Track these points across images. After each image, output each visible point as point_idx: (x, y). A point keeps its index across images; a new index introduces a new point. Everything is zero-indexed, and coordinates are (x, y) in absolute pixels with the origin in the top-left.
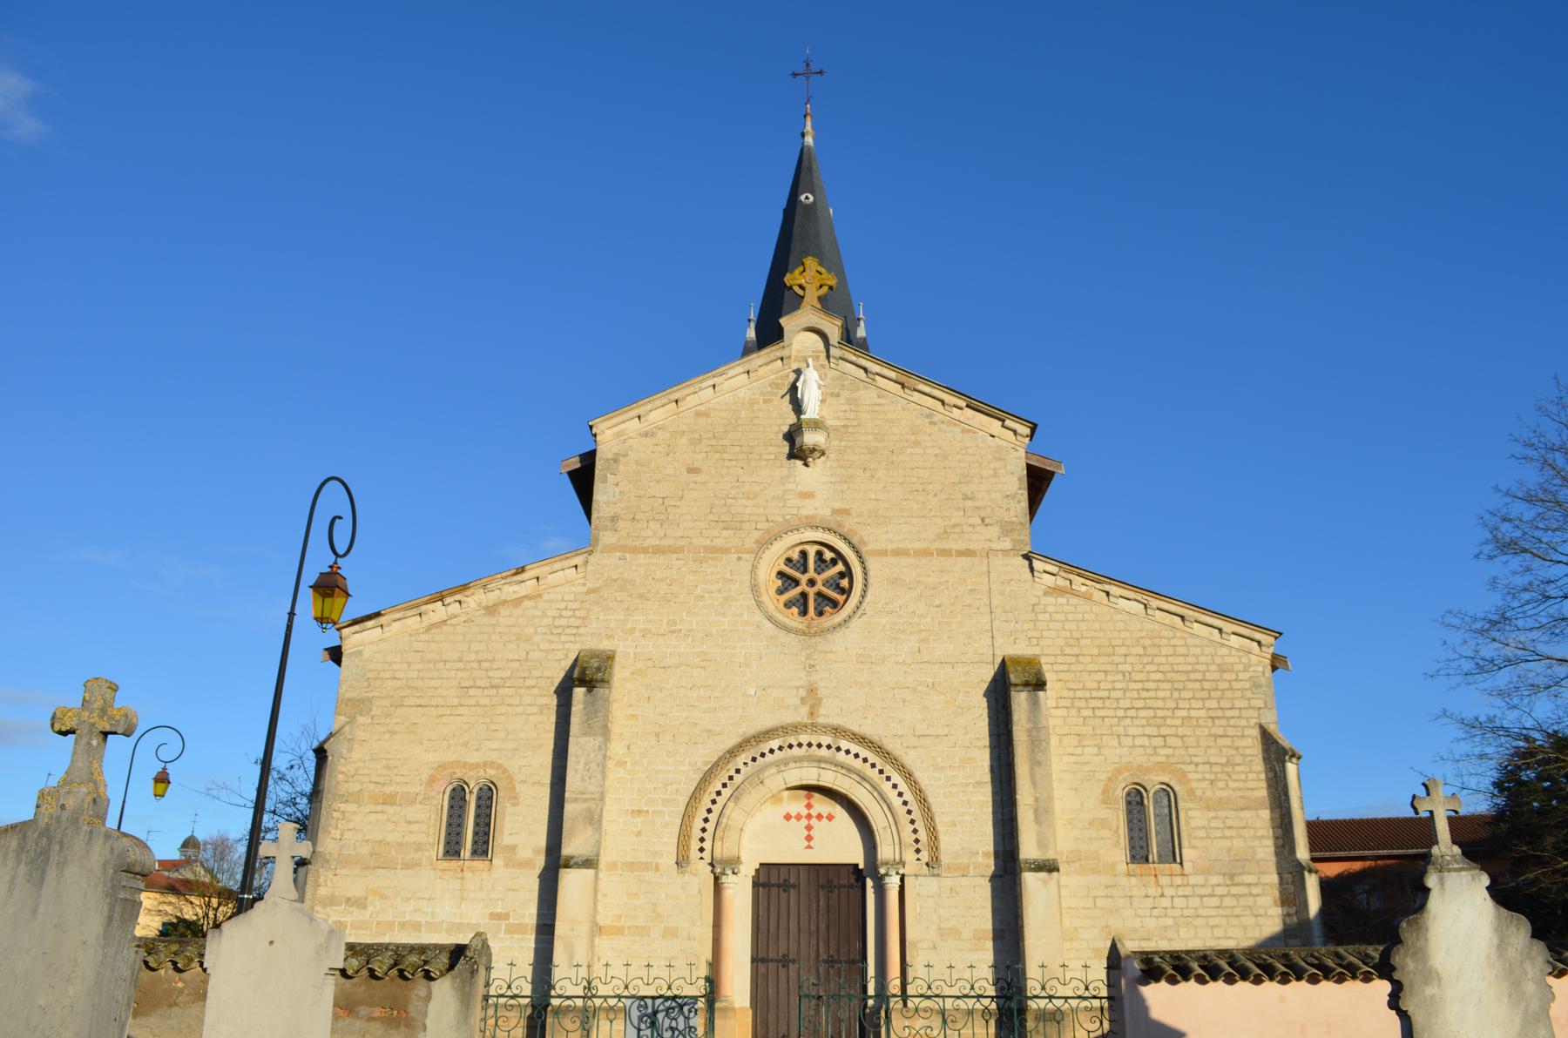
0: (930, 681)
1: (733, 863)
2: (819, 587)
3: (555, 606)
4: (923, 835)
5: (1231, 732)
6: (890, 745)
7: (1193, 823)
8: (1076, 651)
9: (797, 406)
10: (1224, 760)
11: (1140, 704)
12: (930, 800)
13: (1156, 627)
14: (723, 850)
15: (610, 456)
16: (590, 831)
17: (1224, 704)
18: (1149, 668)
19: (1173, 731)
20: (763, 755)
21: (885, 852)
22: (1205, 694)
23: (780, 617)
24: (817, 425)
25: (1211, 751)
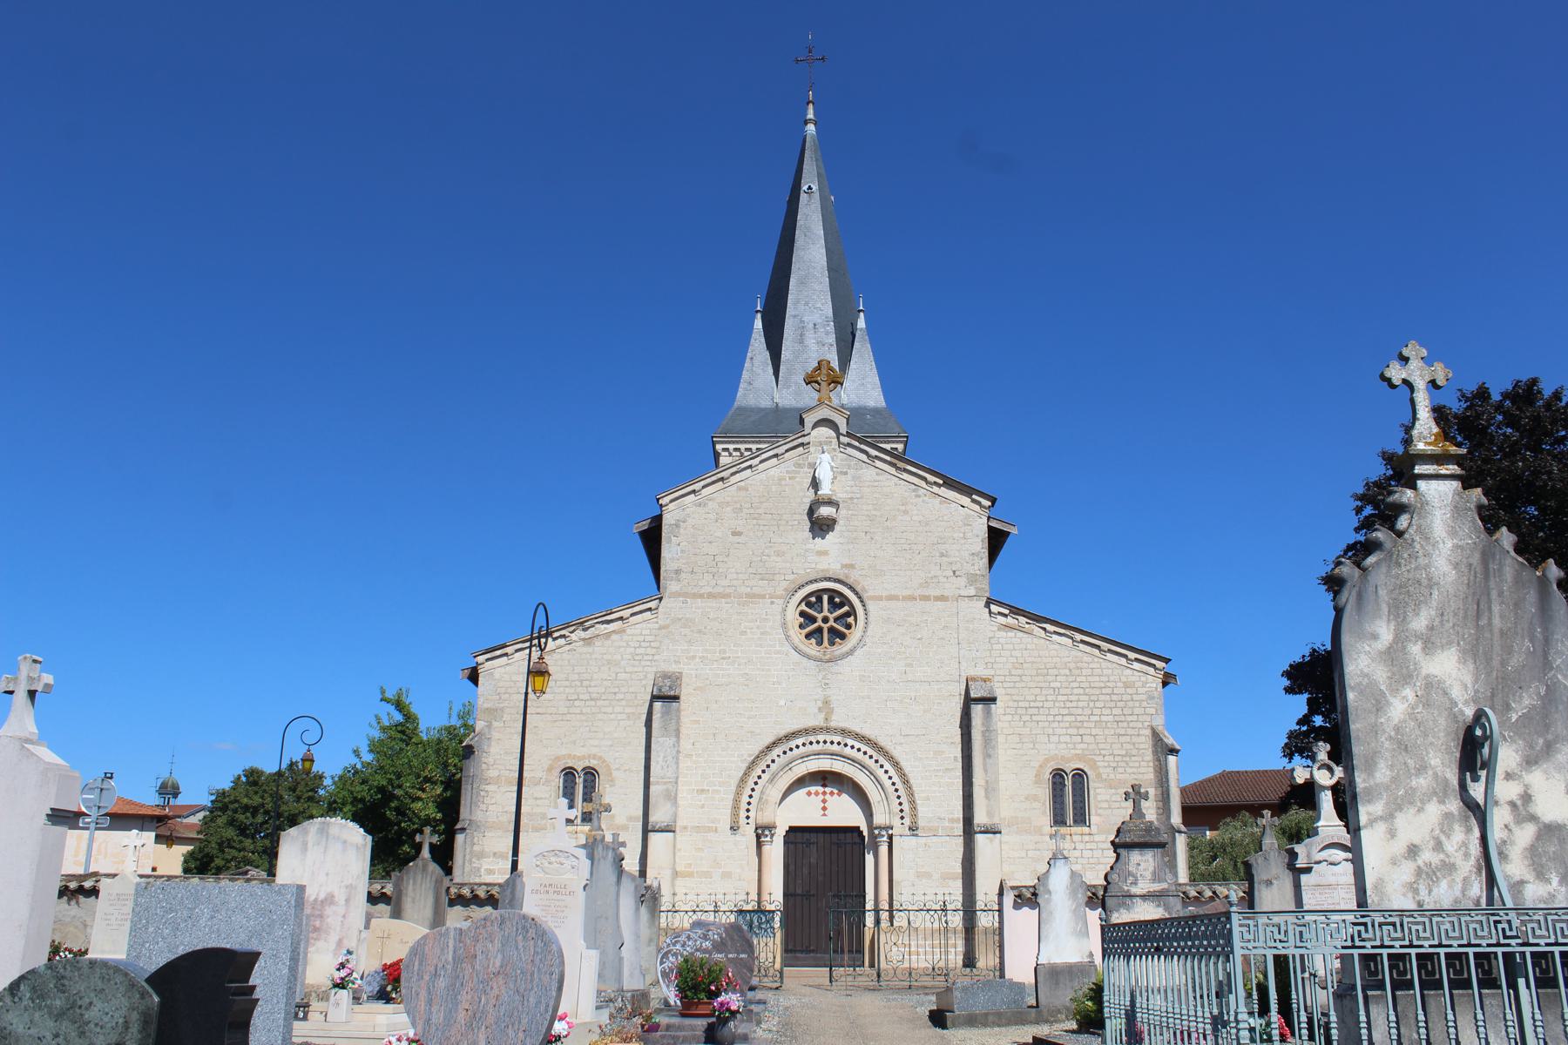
1: (771, 827)
2: (831, 623)
4: (906, 807)
5: (1130, 731)
6: (882, 742)
8: (1020, 672)
9: (815, 484)
14: (765, 819)
16: (669, 805)
21: (879, 819)
24: (830, 502)
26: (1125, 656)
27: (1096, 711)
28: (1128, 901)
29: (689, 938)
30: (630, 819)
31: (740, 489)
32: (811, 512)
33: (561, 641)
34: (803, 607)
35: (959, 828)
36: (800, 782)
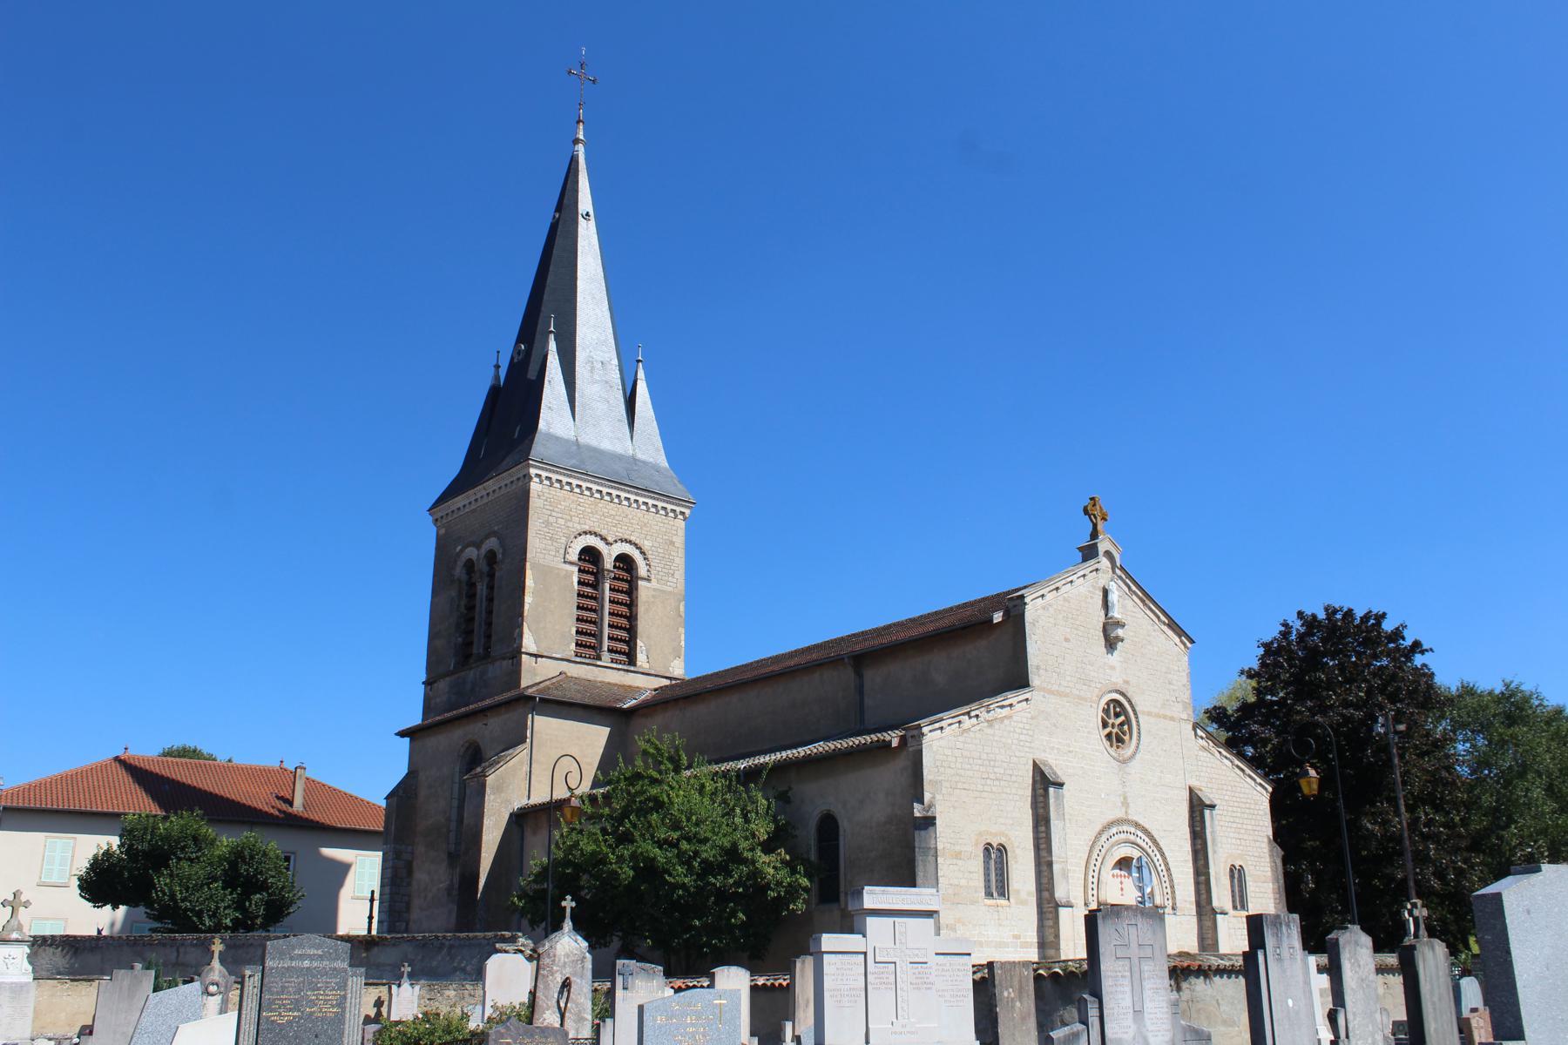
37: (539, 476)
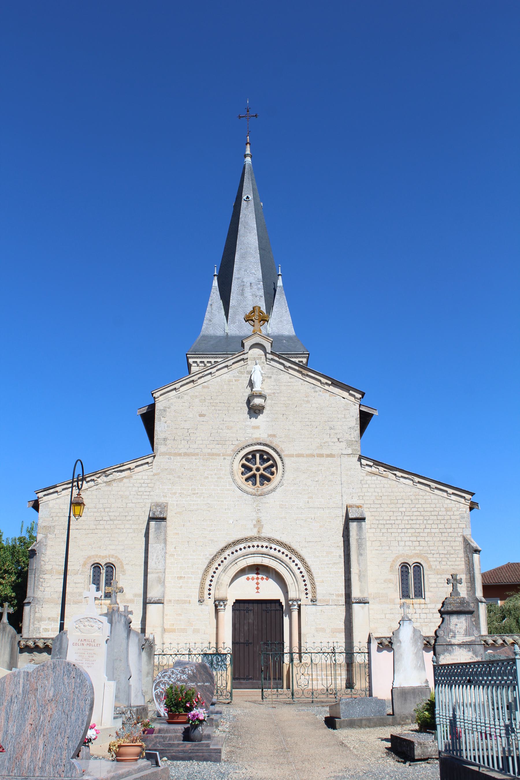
0: (313, 516)
2: (261, 471)
3: (138, 481)
4: (309, 587)
5: (449, 539)
6: (294, 546)
7: (430, 581)
8: (380, 502)
9: (251, 384)
10: (446, 552)
11: (409, 526)
12: (312, 571)
13: (418, 490)
14: (220, 595)
15: (162, 408)
17: (447, 526)
18: (414, 510)
19: (423, 539)
20: (237, 551)
21: (292, 595)
22: (439, 522)
23: (244, 487)
24: (261, 396)
25: (440, 548)
26: (446, 492)
27: (428, 526)
28: (450, 648)
29: (173, 673)
30: (135, 595)
31: (204, 387)
32: (249, 402)
33: (92, 483)
34: (244, 461)
35: (343, 599)
36: (243, 572)
37: (196, 362)
